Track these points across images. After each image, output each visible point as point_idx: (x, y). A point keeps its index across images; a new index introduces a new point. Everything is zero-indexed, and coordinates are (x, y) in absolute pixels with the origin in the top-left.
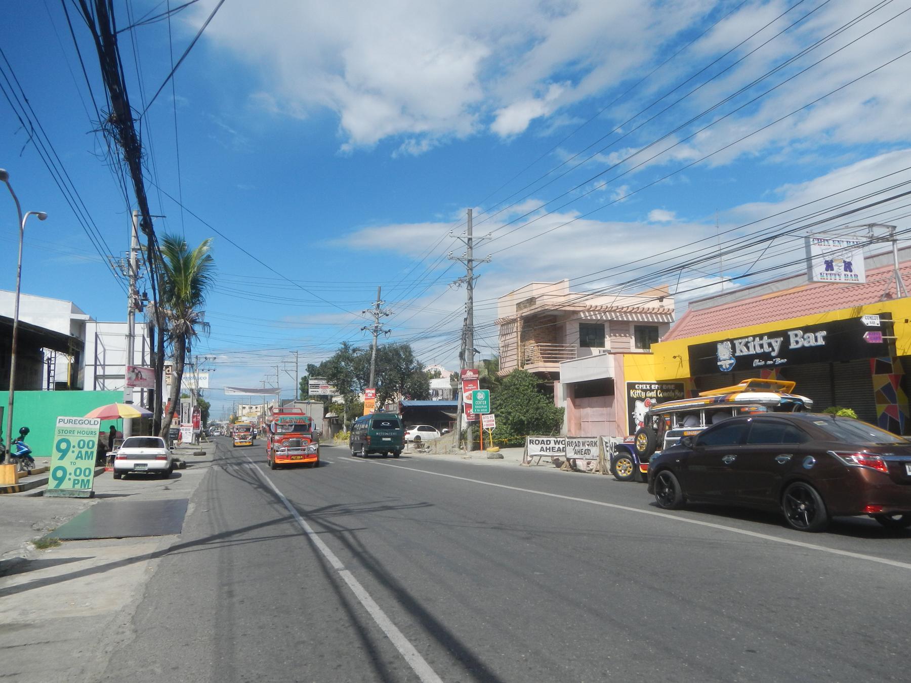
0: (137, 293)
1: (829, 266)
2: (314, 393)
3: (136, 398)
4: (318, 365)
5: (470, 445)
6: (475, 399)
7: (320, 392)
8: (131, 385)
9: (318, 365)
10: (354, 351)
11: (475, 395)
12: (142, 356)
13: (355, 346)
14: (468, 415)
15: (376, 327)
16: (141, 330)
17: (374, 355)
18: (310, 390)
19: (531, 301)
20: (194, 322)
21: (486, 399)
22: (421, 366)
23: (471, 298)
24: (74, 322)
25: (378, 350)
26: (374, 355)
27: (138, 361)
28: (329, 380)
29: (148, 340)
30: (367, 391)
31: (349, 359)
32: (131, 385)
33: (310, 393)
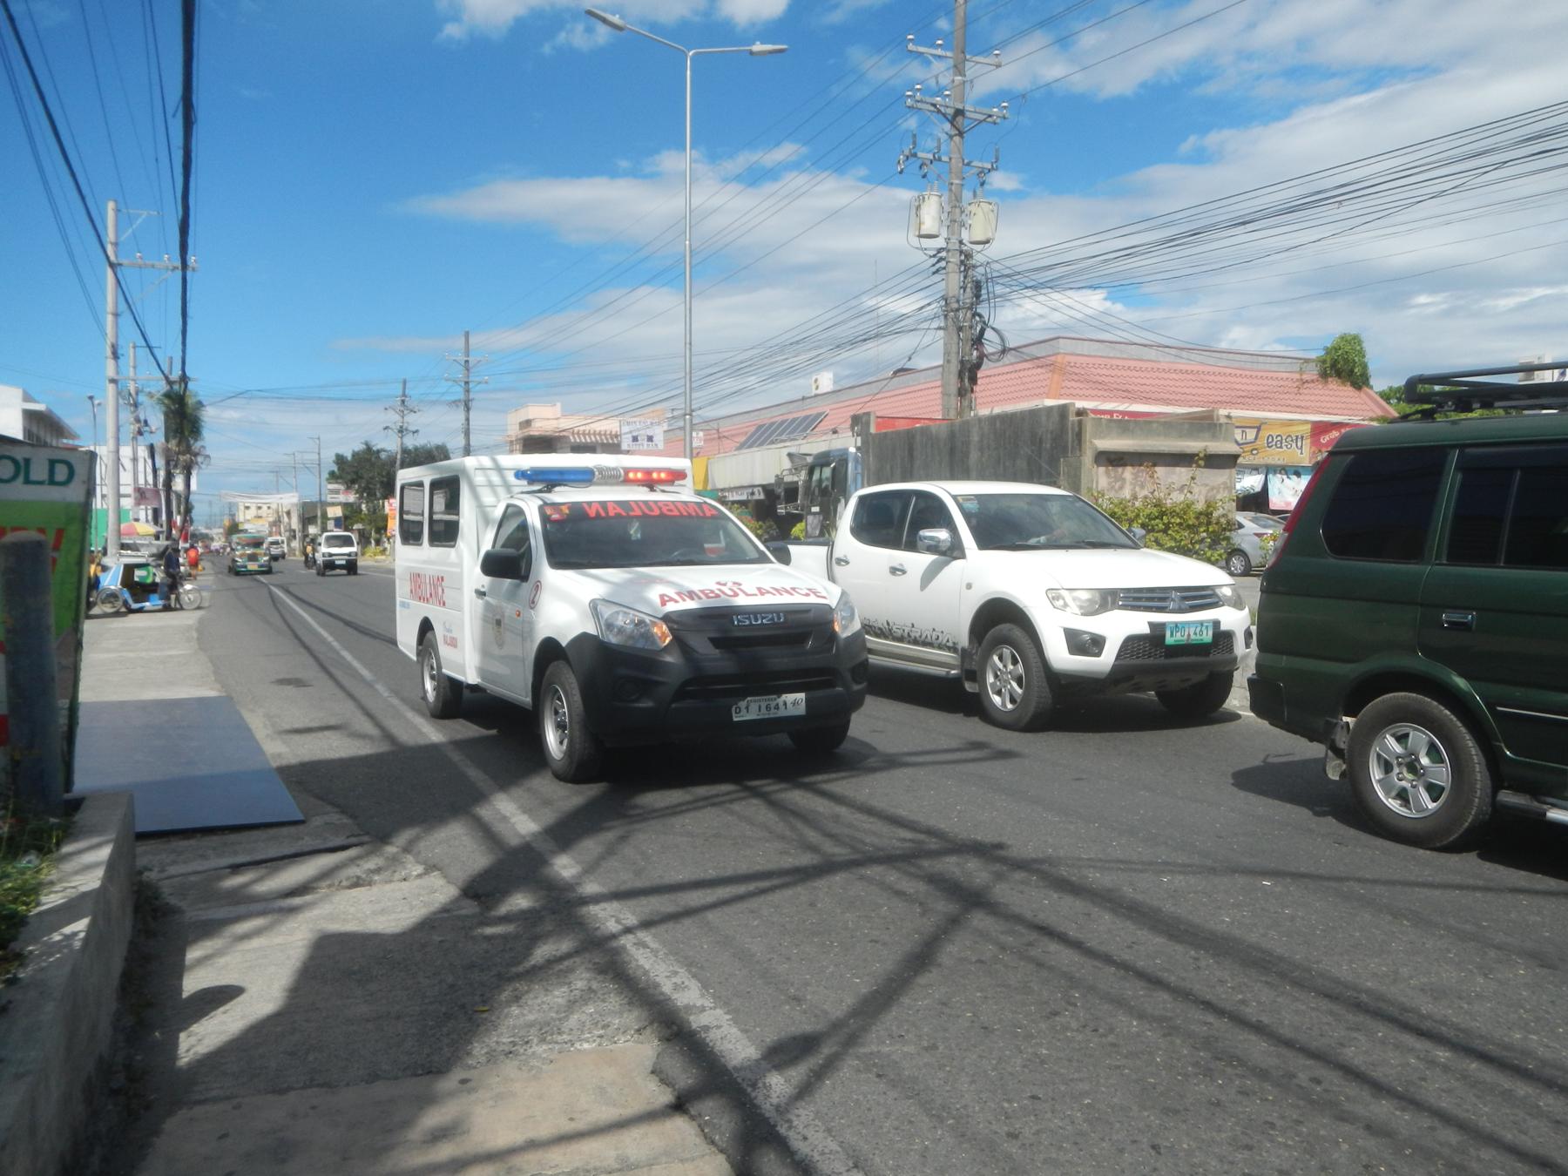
0: (138, 420)
1: (635, 439)
3: (142, 515)
4: (349, 456)
7: (342, 498)
8: (138, 504)
9: (349, 456)
12: (145, 478)
16: (143, 452)
19: (528, 423)
20: (196, 455)
23: (468, 420)
24: (30, 416)
27: (141, 481)
28: (349, 484)
29: (149, 462)
32: (138, 504)
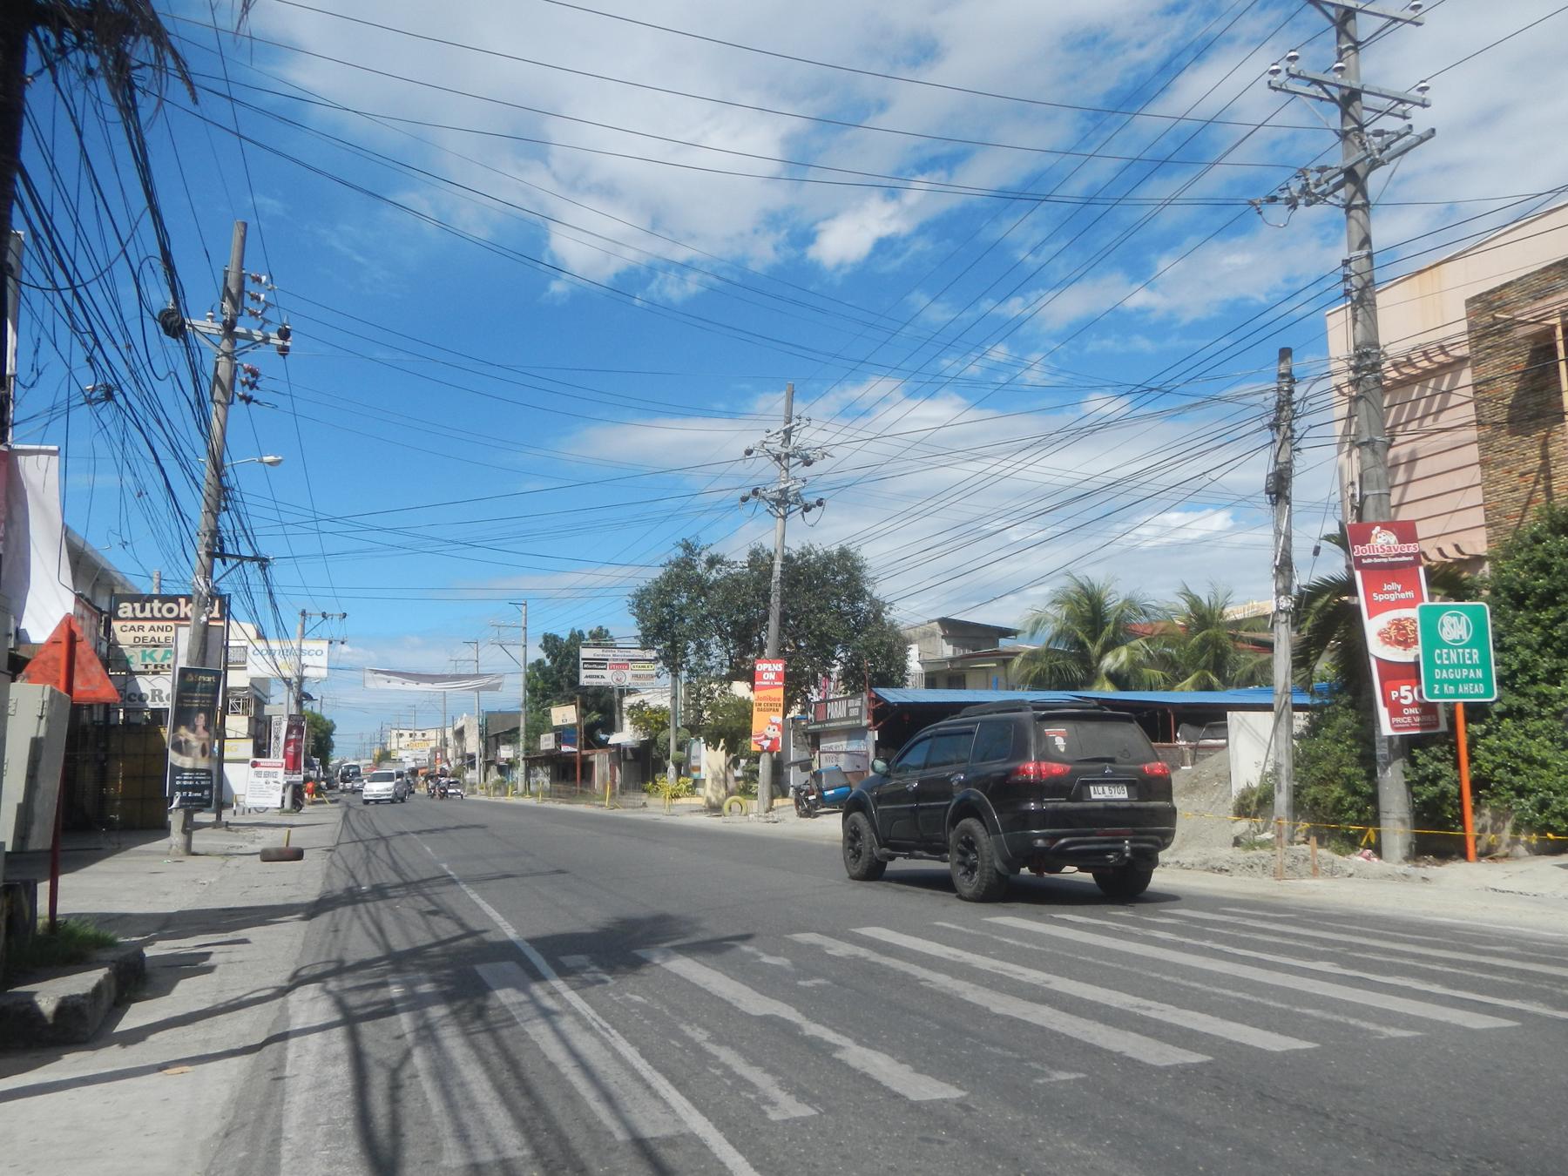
2: (595, 682)
5: (1396, 831)
6: (1433, 641)
10: (712, 562)
11: (1430, 621)
13: (713, 551)
14: (1396, 709)
15: (784, 492)
17: (777, 568)
18: (583, 673)
21: (1476, 641)
22: (878, 607)
25: (787, 559)
26: (777, 568)
30: (760, 667)
31: (701, 587)
33: (584, 681)
